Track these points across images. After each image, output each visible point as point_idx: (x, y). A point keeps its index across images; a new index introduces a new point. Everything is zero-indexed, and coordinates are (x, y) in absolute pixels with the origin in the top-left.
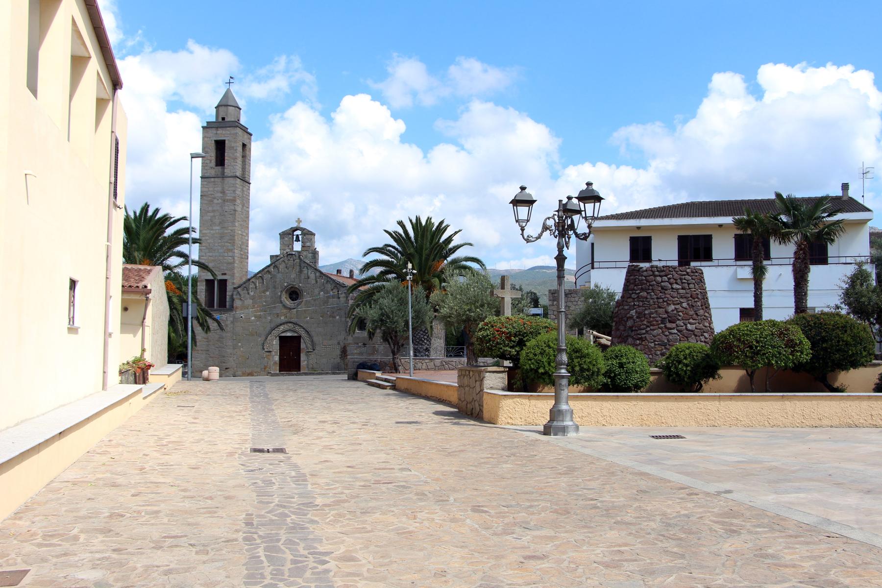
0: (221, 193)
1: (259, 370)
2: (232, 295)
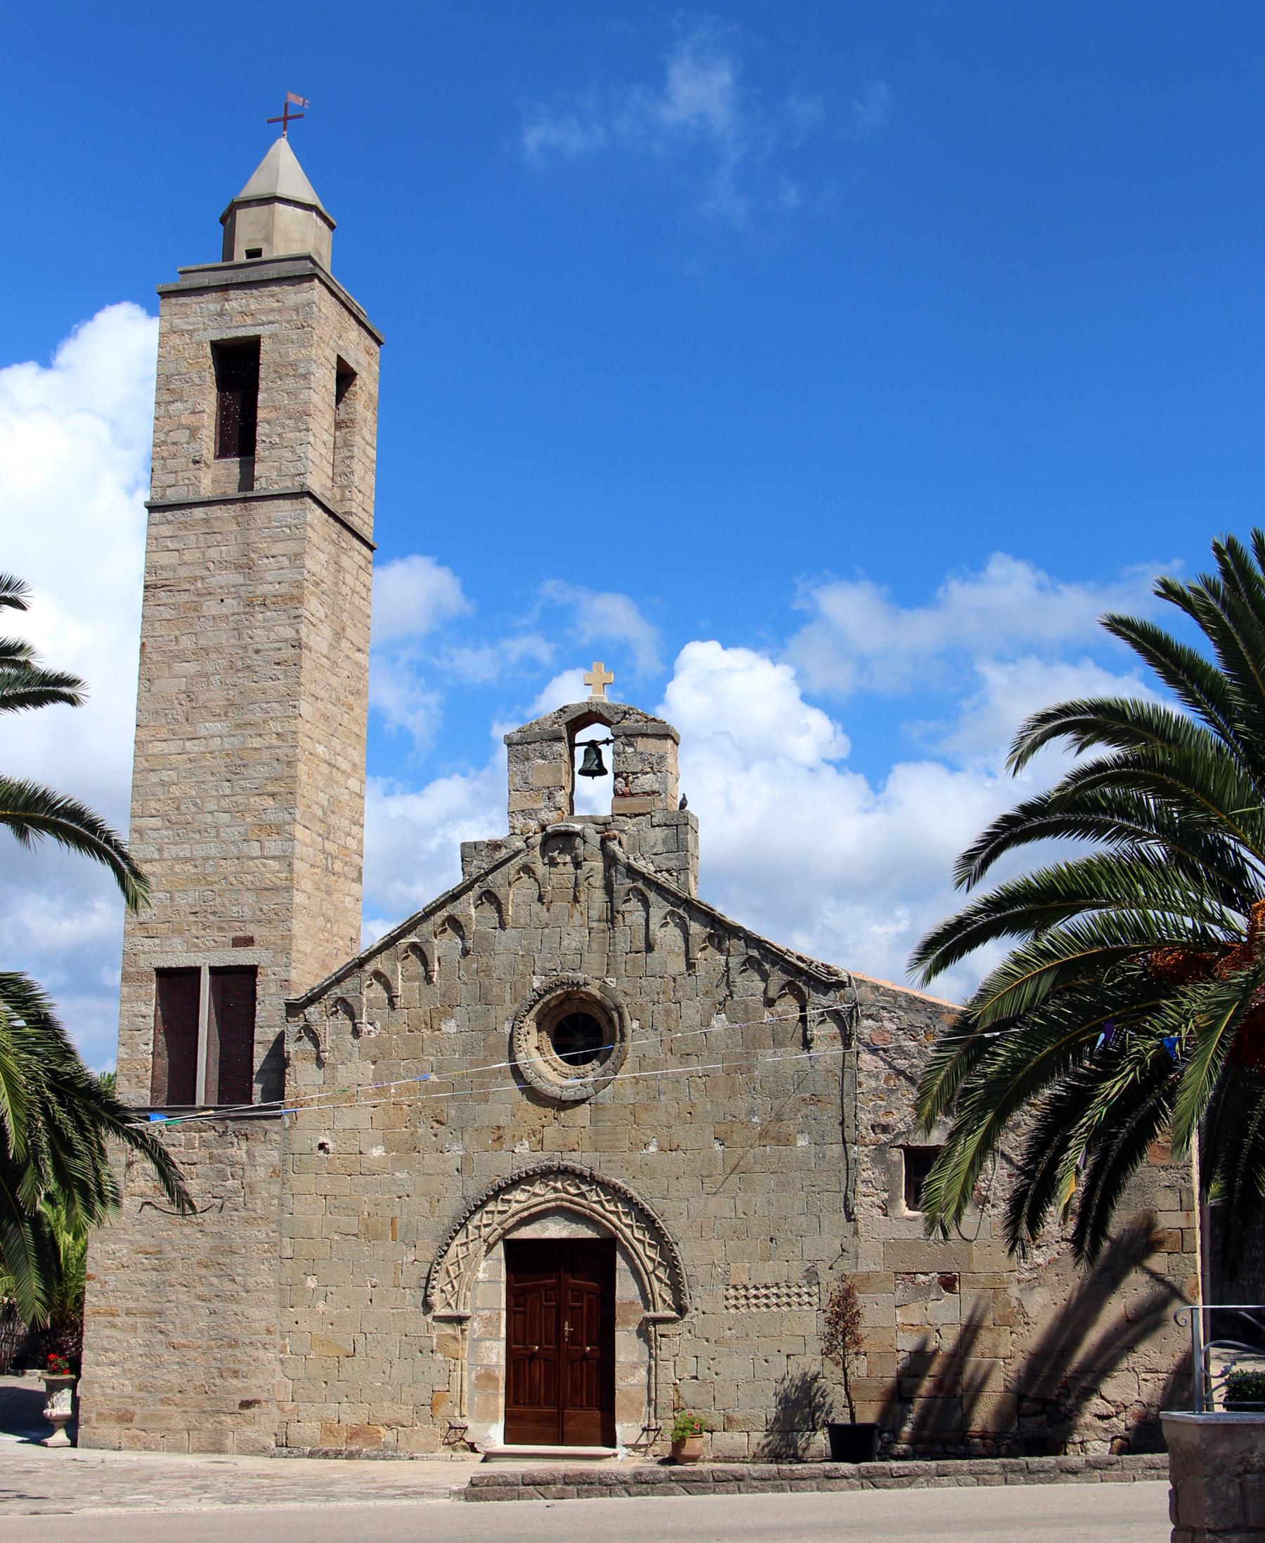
0: (238, 567)
1: (404, 1413)
2: (280, 1040)
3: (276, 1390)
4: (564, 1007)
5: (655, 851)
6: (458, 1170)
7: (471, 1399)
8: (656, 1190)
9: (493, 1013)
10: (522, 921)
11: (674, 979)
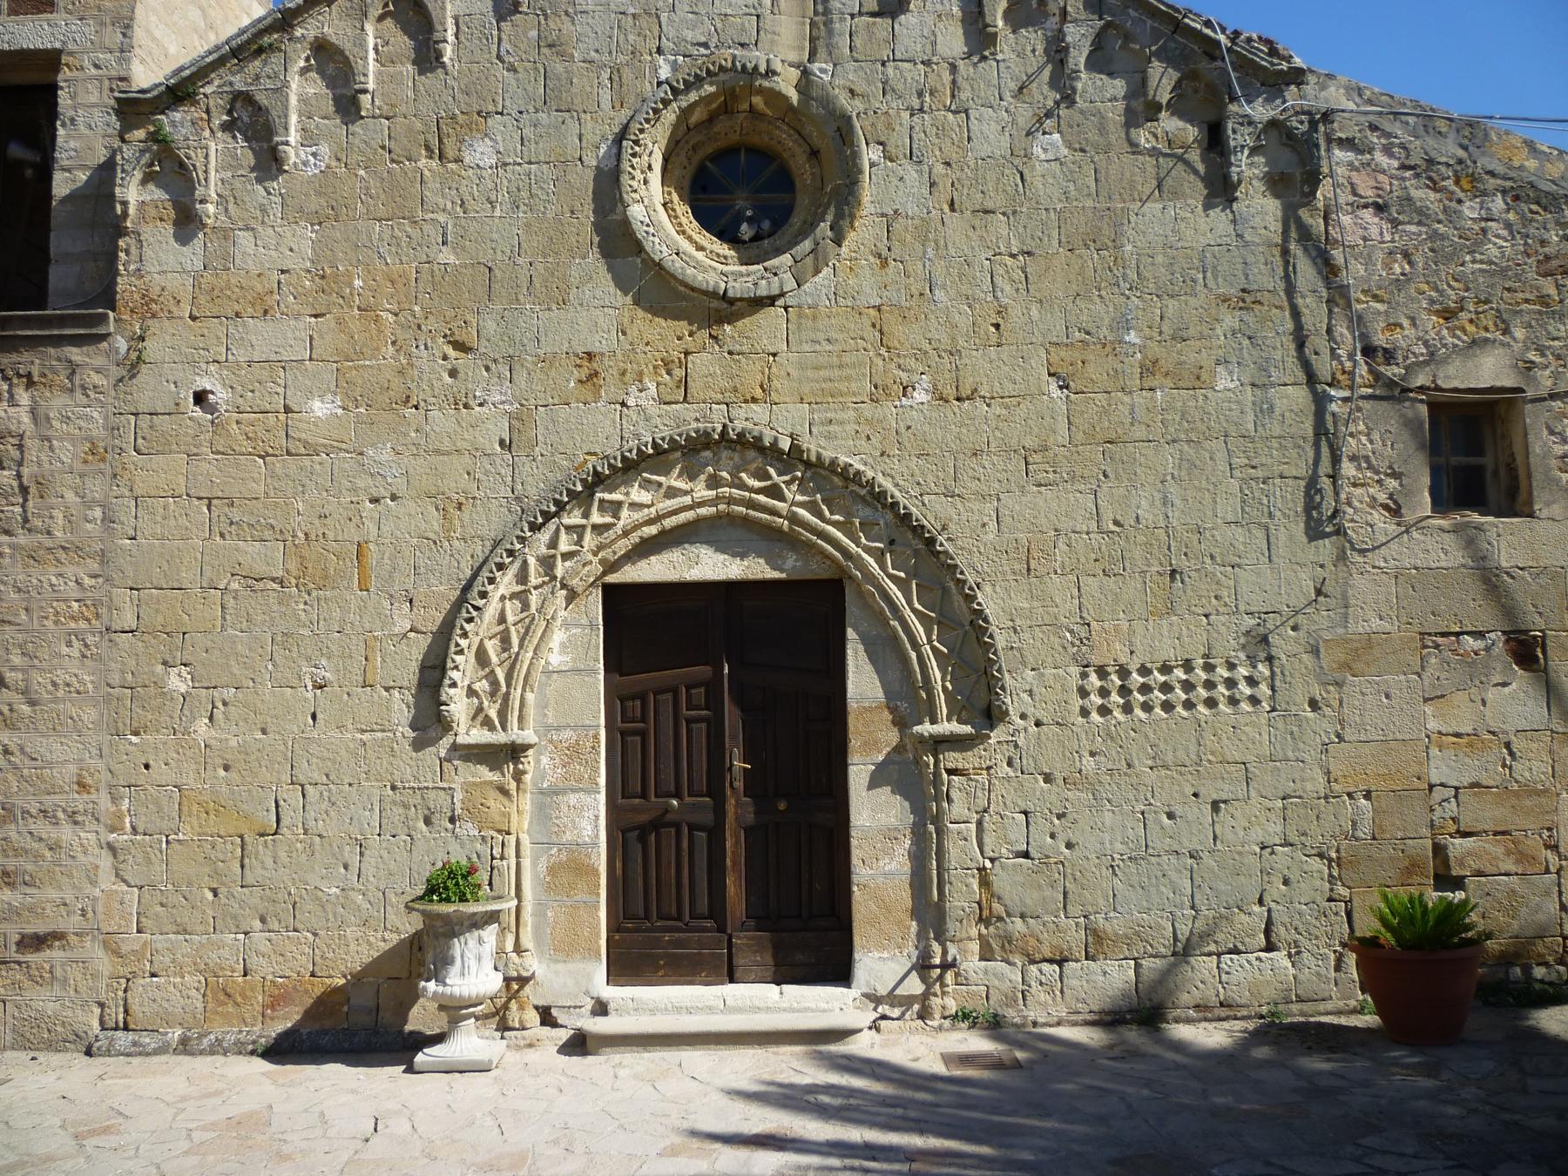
3: (100, 909)
4: (718, 128)
6: (502, 443)
7: (540, 913)
8: (930, 478)
11: (953, 68)
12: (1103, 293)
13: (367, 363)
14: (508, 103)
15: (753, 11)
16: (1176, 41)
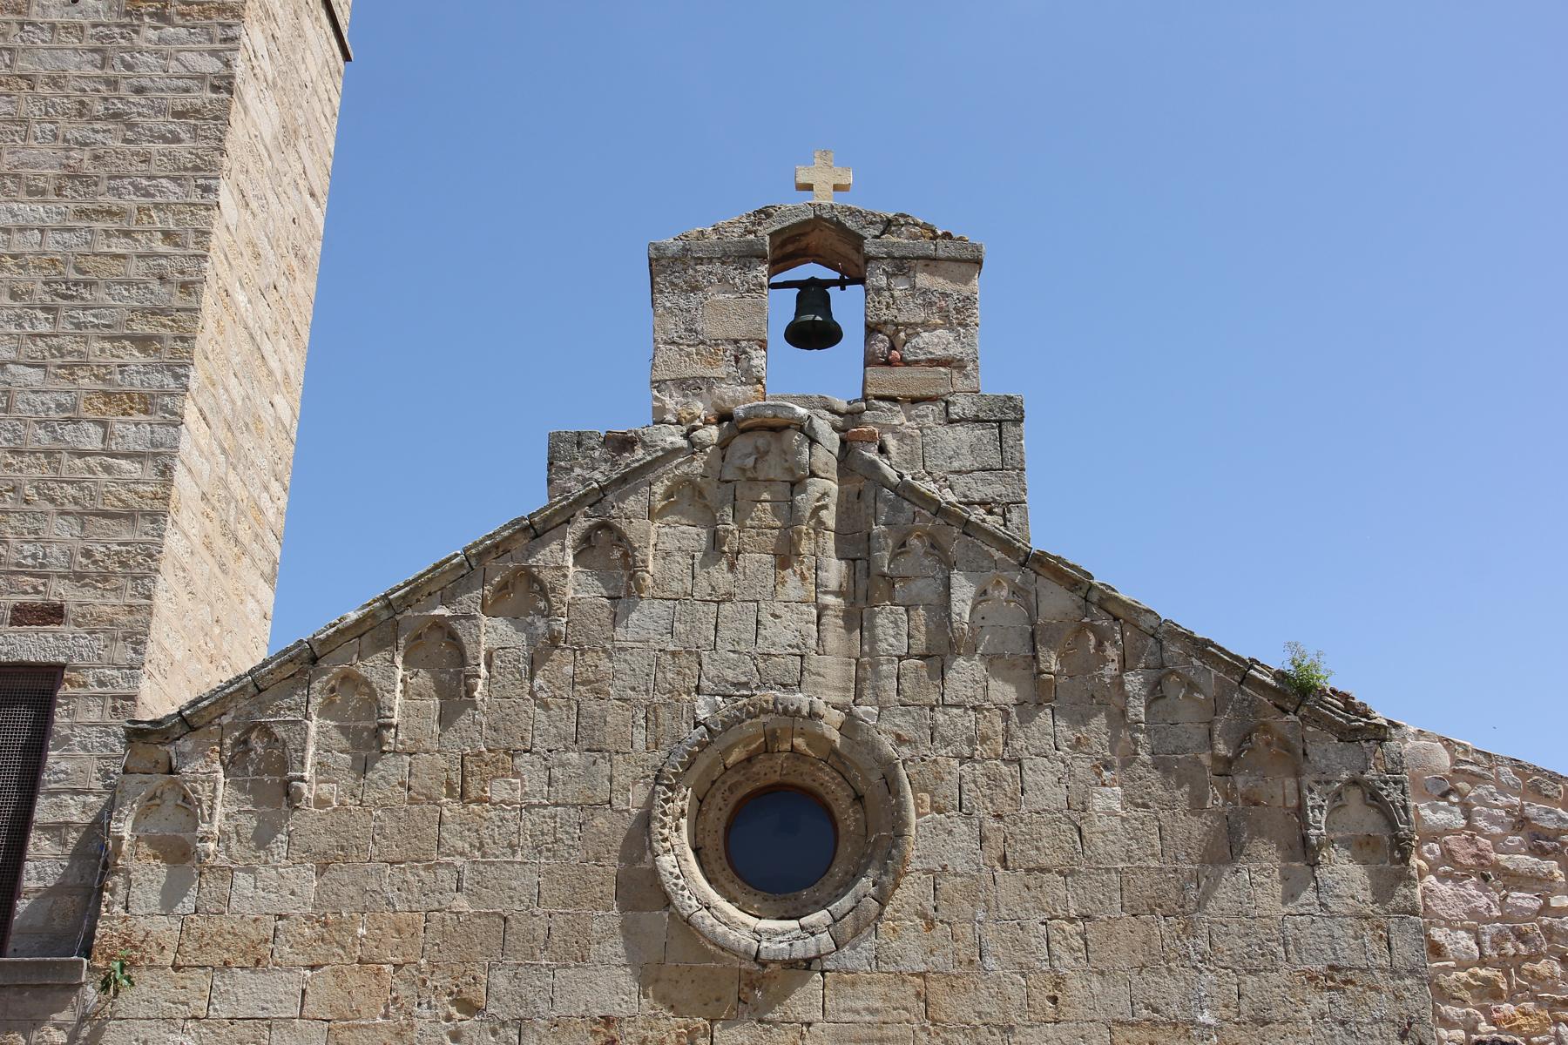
5: (956, 465)
9: (604, 767)
10: (676, 586)
12: (1172, 965)
13: (363, 1022)
14: (537, 740)
15: (797, 652)
16: (1243, 692)
